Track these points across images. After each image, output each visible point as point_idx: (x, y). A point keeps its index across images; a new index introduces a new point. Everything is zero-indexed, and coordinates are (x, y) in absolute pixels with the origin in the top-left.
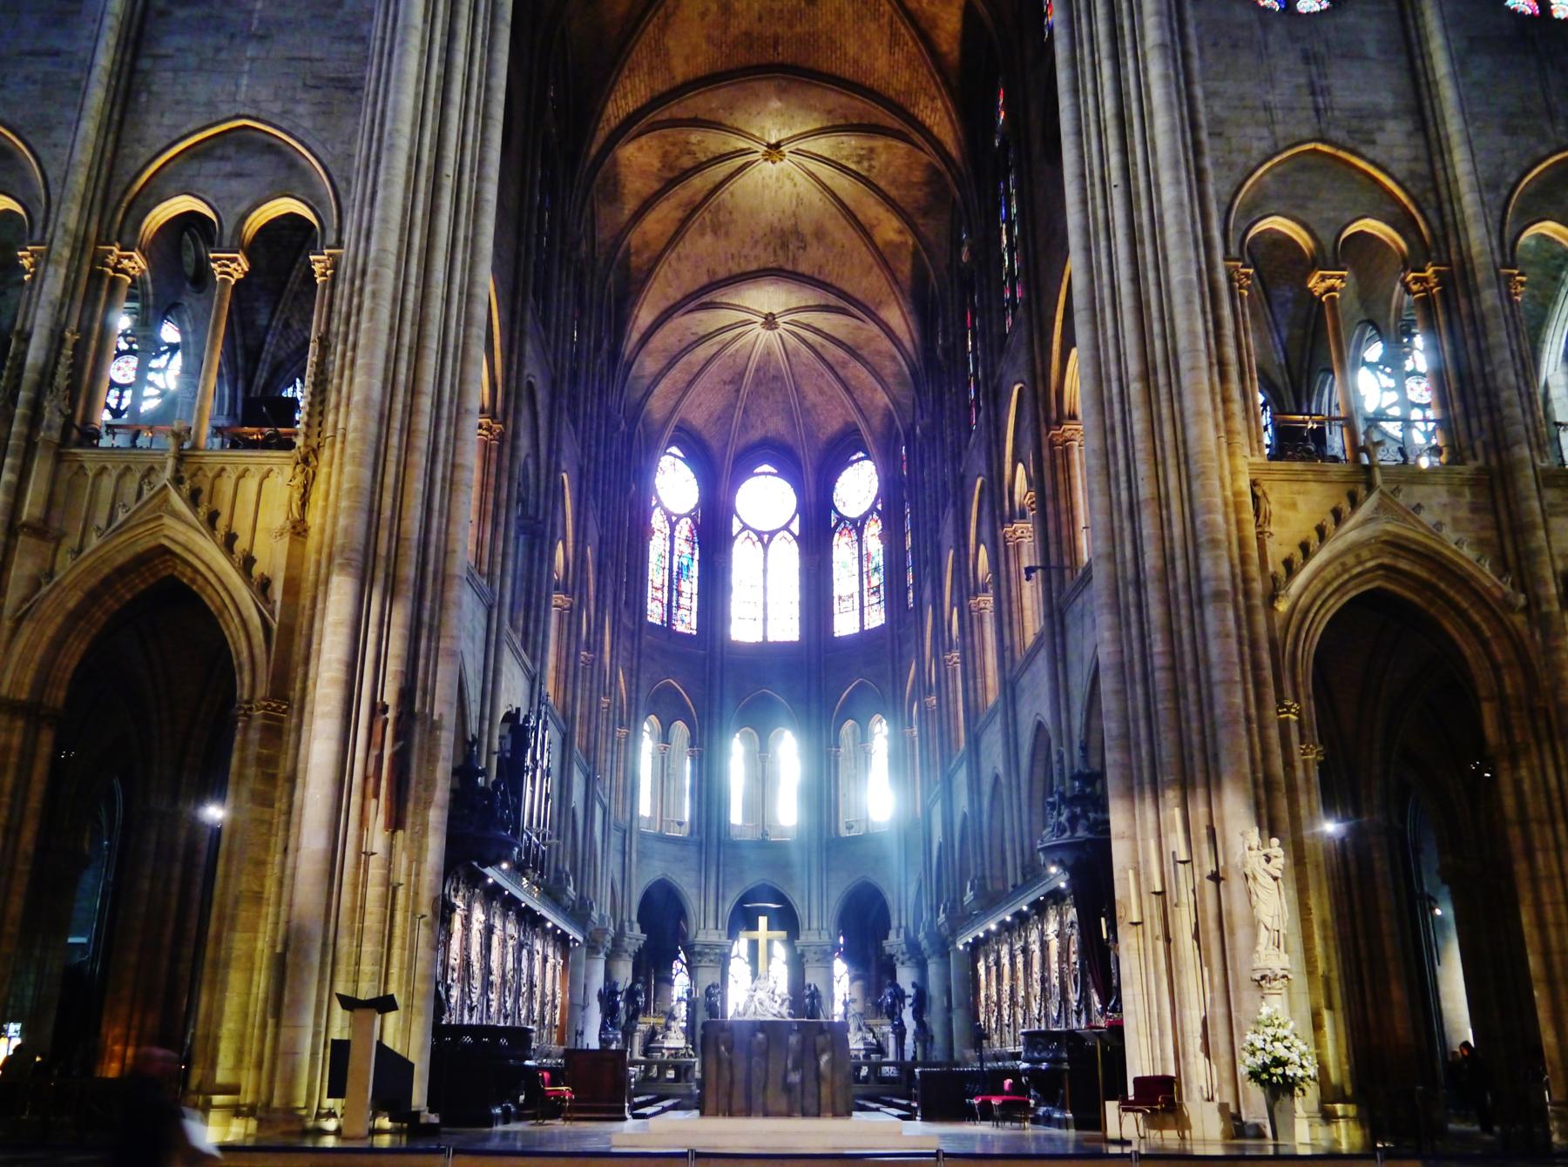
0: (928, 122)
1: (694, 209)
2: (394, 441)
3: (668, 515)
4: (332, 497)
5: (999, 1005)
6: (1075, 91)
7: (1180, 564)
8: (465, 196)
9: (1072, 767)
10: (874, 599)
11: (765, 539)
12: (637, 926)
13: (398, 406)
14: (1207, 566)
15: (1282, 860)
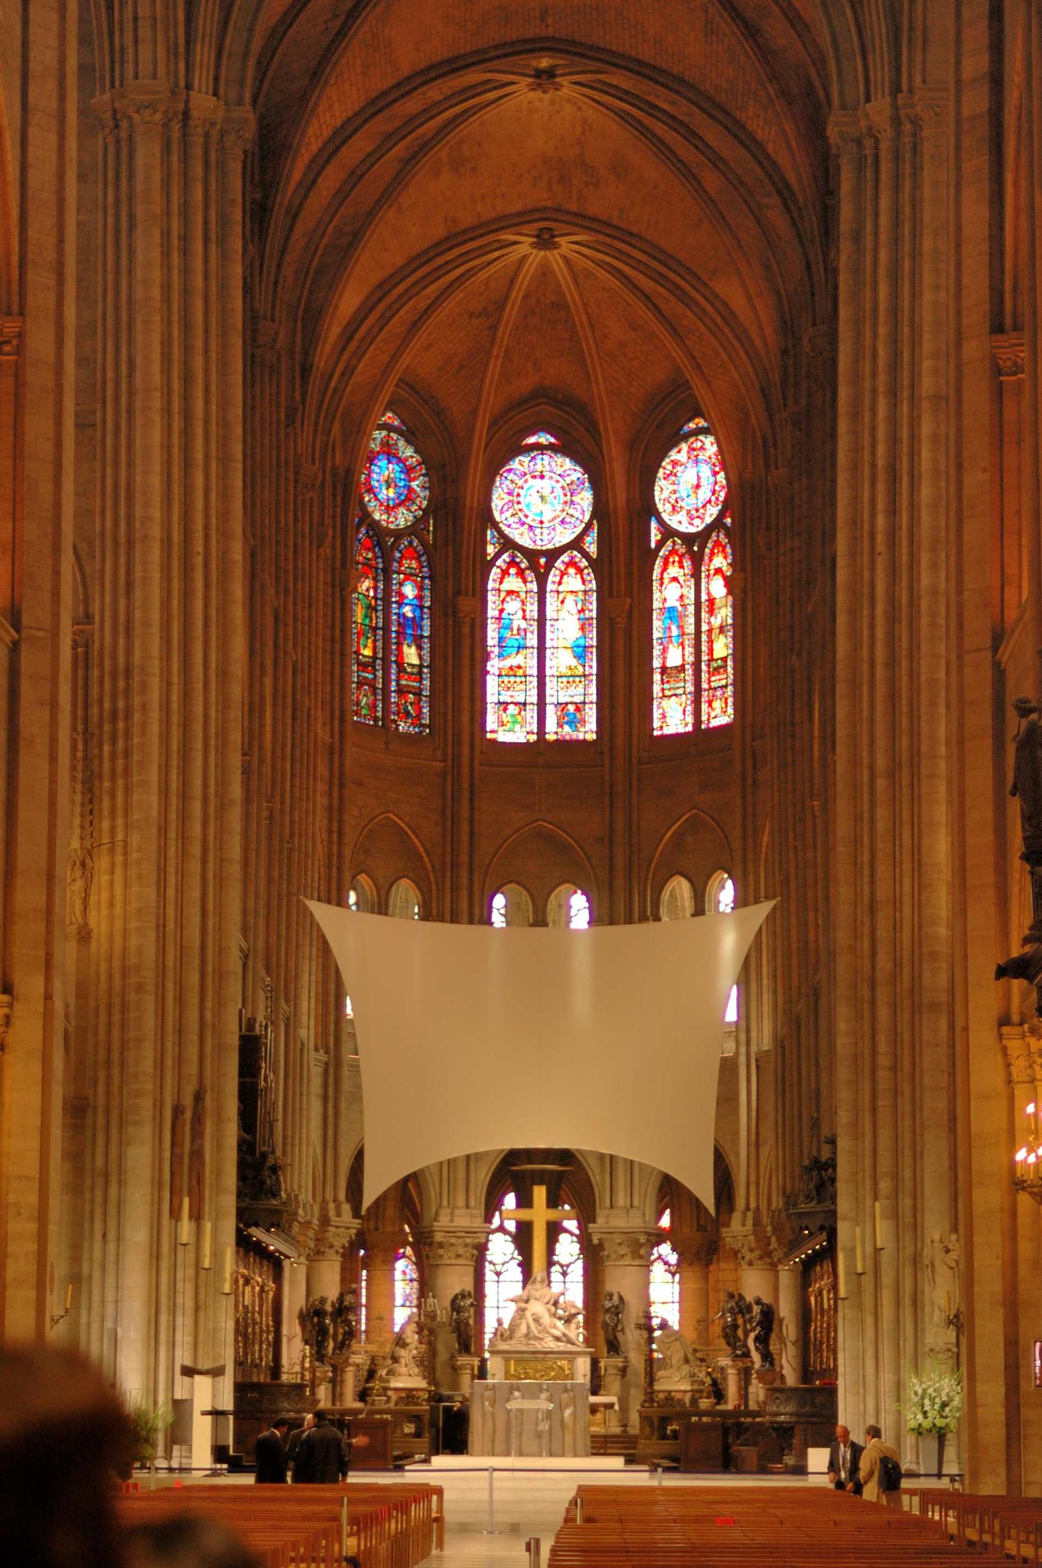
0: (760, 135)
1: (425, 147)
2: (172, 852)
3: (378, 533)
4: (118, 910)
5: (822, 1343)
6: (856, 415)
7: (906, 970)
8: (213, 565)
9: (810, 1152)
10: (718, 681)
11: (538, 564)
12: (346, 1208)
13: (173, 816)
14: (926, 974)
15: (957, 1252)
